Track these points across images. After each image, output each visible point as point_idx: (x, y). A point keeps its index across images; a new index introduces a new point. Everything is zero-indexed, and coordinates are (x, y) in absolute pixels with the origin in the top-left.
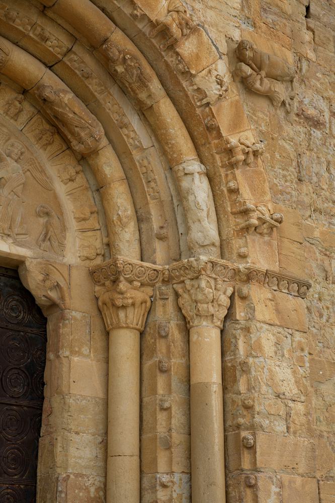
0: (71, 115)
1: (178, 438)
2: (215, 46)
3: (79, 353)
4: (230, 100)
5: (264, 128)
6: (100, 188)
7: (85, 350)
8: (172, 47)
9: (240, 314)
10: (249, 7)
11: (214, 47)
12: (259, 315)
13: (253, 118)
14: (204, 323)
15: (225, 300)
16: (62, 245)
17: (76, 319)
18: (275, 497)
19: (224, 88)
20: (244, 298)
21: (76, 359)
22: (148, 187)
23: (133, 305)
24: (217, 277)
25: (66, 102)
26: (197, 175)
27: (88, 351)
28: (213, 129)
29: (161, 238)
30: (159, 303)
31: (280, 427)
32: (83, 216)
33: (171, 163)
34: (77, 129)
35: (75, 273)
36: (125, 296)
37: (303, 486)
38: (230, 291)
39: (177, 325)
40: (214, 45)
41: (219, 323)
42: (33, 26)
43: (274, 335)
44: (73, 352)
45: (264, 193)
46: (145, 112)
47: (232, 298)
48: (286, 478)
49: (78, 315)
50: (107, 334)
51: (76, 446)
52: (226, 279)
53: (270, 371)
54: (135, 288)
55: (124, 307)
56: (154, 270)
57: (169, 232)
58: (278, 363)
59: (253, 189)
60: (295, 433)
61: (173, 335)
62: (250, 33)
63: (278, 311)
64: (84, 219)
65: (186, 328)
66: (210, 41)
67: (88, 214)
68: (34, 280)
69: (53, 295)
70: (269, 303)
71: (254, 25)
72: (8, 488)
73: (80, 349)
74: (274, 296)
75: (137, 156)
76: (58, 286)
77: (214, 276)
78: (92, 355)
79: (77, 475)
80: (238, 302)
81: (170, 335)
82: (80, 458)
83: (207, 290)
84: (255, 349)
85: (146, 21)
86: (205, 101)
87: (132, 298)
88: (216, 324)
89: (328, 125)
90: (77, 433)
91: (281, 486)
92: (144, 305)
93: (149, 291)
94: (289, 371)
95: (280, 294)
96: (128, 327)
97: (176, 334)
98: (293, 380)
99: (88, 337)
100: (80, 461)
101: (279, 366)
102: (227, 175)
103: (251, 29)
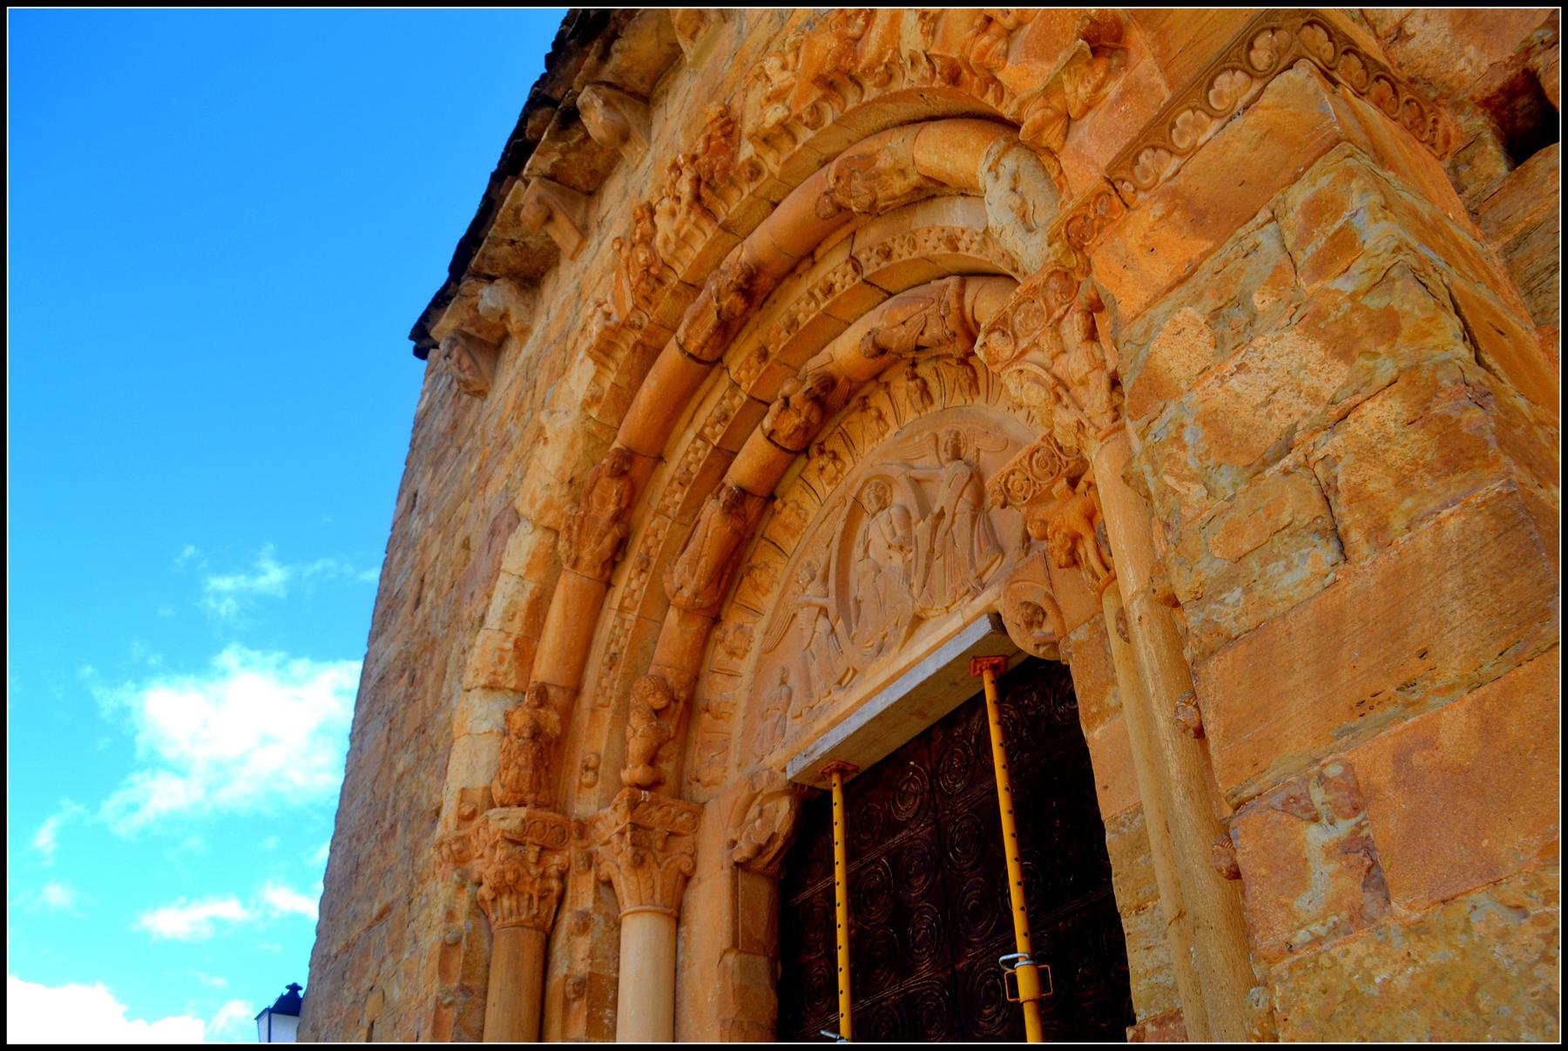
18: (1333, 866)
37: (1488, 729)
51: (1143, 943)
60: (1379, 531)
73: (1100, 703)
82: (1159, 969)
90: (1140, 909)
100: (1161, 979)
101: (1240, 367)
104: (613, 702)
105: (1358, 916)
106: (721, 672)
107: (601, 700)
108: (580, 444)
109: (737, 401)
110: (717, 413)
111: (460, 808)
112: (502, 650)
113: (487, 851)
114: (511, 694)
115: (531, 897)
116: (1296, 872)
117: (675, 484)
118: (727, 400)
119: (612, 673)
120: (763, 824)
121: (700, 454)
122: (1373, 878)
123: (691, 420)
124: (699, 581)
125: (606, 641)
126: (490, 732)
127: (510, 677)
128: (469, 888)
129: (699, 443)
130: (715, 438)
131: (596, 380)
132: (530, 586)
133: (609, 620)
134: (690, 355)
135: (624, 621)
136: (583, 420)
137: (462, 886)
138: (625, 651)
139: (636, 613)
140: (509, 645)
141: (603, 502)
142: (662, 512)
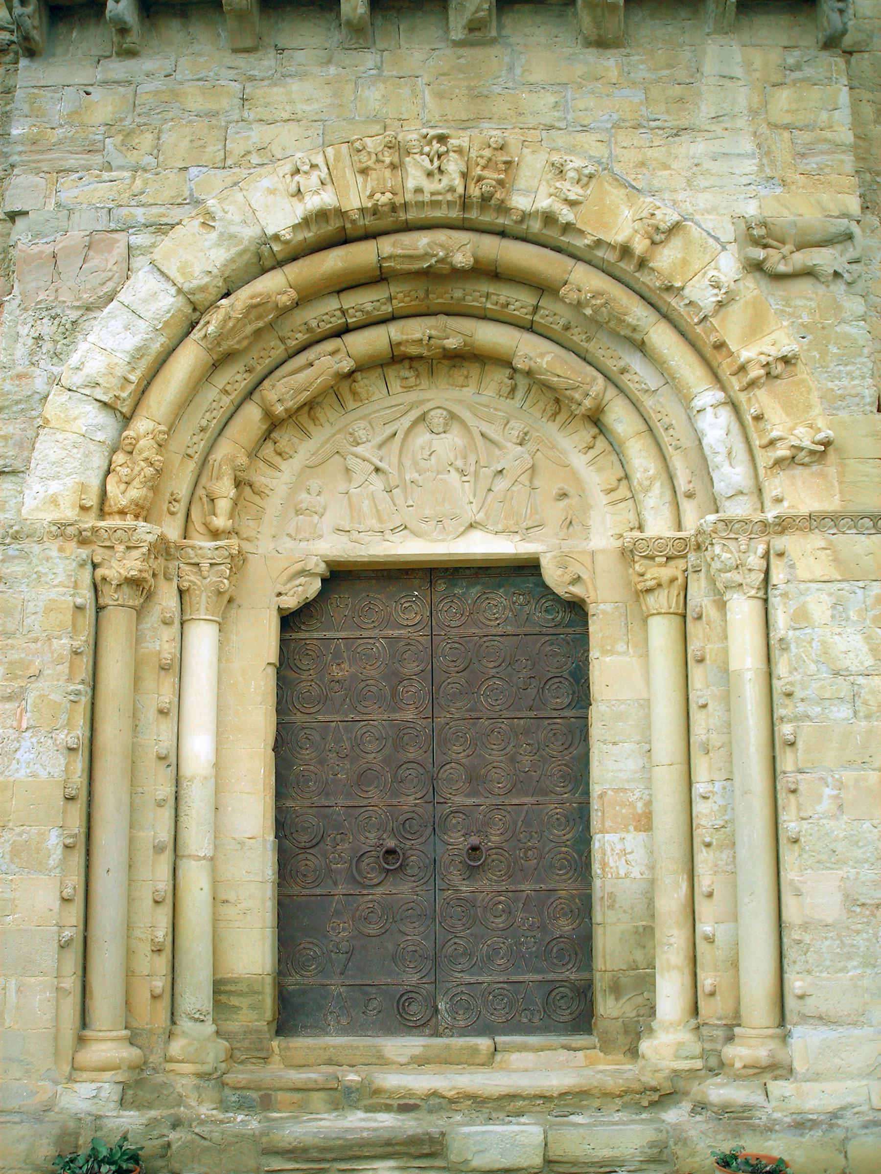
0: (555, 379)
1: (716, 739)
2: (712, 236)
3: (612, 652)
4: (742, 301)
5: (806, 319)
6: (617, 449)
7: (621, 647)
8: (642, 264)
9: (778, 576)
10: (773, 163)
11: (711, 241)
12: (802, 573)
13: (785, 311)
14: (735, 596)
15: (755, 561)
16: (586, 527)
17: (604, 613)
18: (830, 801)
19: (723, 291)
20: (781, 555)
21: (608, 659)
22: (667, 436)
23: (659, 585)
24: (737, 536)
25: (545, 366)
26: (709, 410)
27: (625, 647)
28: (720, 346)
29: (690, 496)
30: (692, 578)
31: (843, 712)
32: (610, 487)
33: (685, 399)
34: (568, 393)
35: (599, 558)
36: (645, 578)
38: (761, 549)
39: (714, 601)
40: (712, 236)
41: (753, 592)
42: (488, 296)
43: (830, 595)
44: (605, 652)
45: (809, 407)
46: (641, 347)
47: (766, 556)
48: (848, 776)
49: (608, 607)
50: (645, 620)
51: (614, 758)
52: (753, 536)
53: (824, 643)
54: (660, 565)
55: (649, 591)
56: (680, 539)
57: (697, 486)
58: (839, 630)
59: (788, 407)
61: (707, 615)
62: (777, 198)
63: (837, 560)
64: (612, 490)
65: (722, 606)
66: (704, 234)
67: (615, 483)
68: (552, 575)
69: (577, 590)
70: (822, 554)
71: (784, 183)
72: (556, 808)
74: (830, 542)
75: (648, 402)
76: (578, 580)
77: (733, 536)
78: (631, 651)
79: (617, 791)
80: (773, 560)
81: (704, 615)
82: (620, 771)
83: (725, 555)
84: (801, 618)
85: (605, 246)
86: (702, 315)
87: (654, 578)
88: (749, 595)
89: (17, 616)
90: (614, 744)
91: (840, 786)
92: (676, 582)
93: (681, 564)
94: (859, 637)
95: (840, 537)
96: (659, 614)
97: (711, 612)
98: (866, 648)
99: (624, 630)
100: (620, 775)
101: (840, 634)
102: (749, 399)
103: (779, 190)
104: (197, 456)
105: (834, 817)
106: (265, 461)
107: (190, 452)
108: (246, 257)
109: (384, 308)
110: (369, 307)
111: (81, 499)
112: (126, 380)
113: (121, 548)
114: (118, 415)
115: (143, 588)
116: (819, 799)
117: (304, 328)
118: (378, 303)
119: (202, 434)
120: (304, 591)
121: (333, 319)
122: (840, 807)
123: (339, 292)
124: (295, 404)
125: (205, 409)
126: (104, 442)
127: (127, 403)
128: (89, 567)
129: (338, 313)
130: (351, 318)
131: (295, 227)
132: (162, 339)
133: (211, 394)
134: (381, 267)
135: (220, 399)
136: (259, 241)
137: (82, 565)
138: (215, 421)
139: (231, 397)
140: (133, 378)
141: (258, 318)
142: (282, 340)
